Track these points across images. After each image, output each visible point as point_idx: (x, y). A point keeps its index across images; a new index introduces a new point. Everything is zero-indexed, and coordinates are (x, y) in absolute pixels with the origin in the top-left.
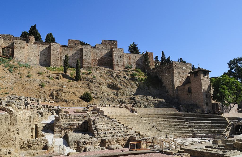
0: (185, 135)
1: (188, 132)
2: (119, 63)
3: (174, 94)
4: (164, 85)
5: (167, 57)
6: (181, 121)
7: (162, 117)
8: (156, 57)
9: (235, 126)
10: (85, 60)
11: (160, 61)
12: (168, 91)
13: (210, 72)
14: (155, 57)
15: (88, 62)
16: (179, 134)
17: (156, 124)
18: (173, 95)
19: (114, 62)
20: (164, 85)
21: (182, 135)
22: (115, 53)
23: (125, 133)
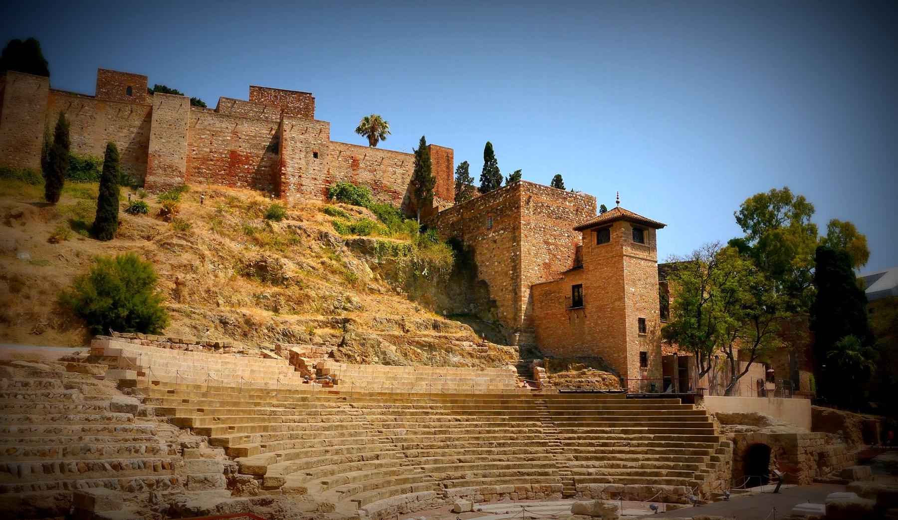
0: (528, 486)
1: (546, 474)
2: (305, 181)
4: (481, 277)
5: (506, 172)
6: (523, 426)
7: (445, 408)
8: (464, 167)
9: (743, 448)
10: (160, 156)
11: (477, 184)
12: (495, 301)
13: (661, 226)
14: (459, 167)
15: (169, 167)
19: (284, 174)
20: (481, 277)
21: (519, 488)
22: (293, 138)
23: (151, 471)
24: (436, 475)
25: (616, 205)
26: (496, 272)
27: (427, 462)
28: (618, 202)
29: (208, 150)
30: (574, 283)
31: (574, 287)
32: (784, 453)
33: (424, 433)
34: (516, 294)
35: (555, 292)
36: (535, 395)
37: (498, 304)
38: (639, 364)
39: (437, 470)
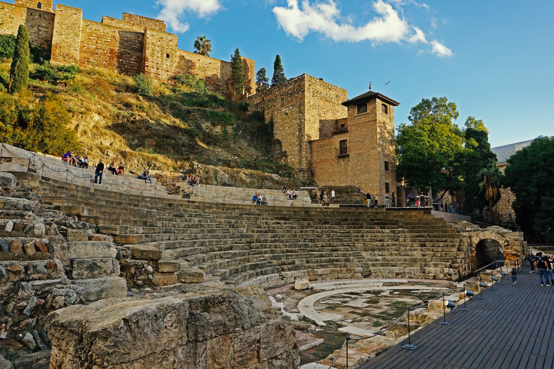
0: (339, 269)
3: (301, 159)
4: (276, 137)
8: (262, 72)
9: (477, 242)
10: (60, 47)
12: (286, 152)
14: (259, 72)
16: (322, 266)
17: (250, 233)
18: (300, 163)
21: (333, 271)
22: (153, 44)
24: (275, 262)
25: (369, 90)
26: (286, 134)
27: (266, 252)
28: (370, 88)
29: (94, 47)
30: (341, 139)
31: (341, 141)
32: (508, 245)
33: (258, 232)
34: (301, 147)
35: (327, 145)
36: (325, 208)
37: (288, 154)
38: (385, 191)
39: (273, 258)
